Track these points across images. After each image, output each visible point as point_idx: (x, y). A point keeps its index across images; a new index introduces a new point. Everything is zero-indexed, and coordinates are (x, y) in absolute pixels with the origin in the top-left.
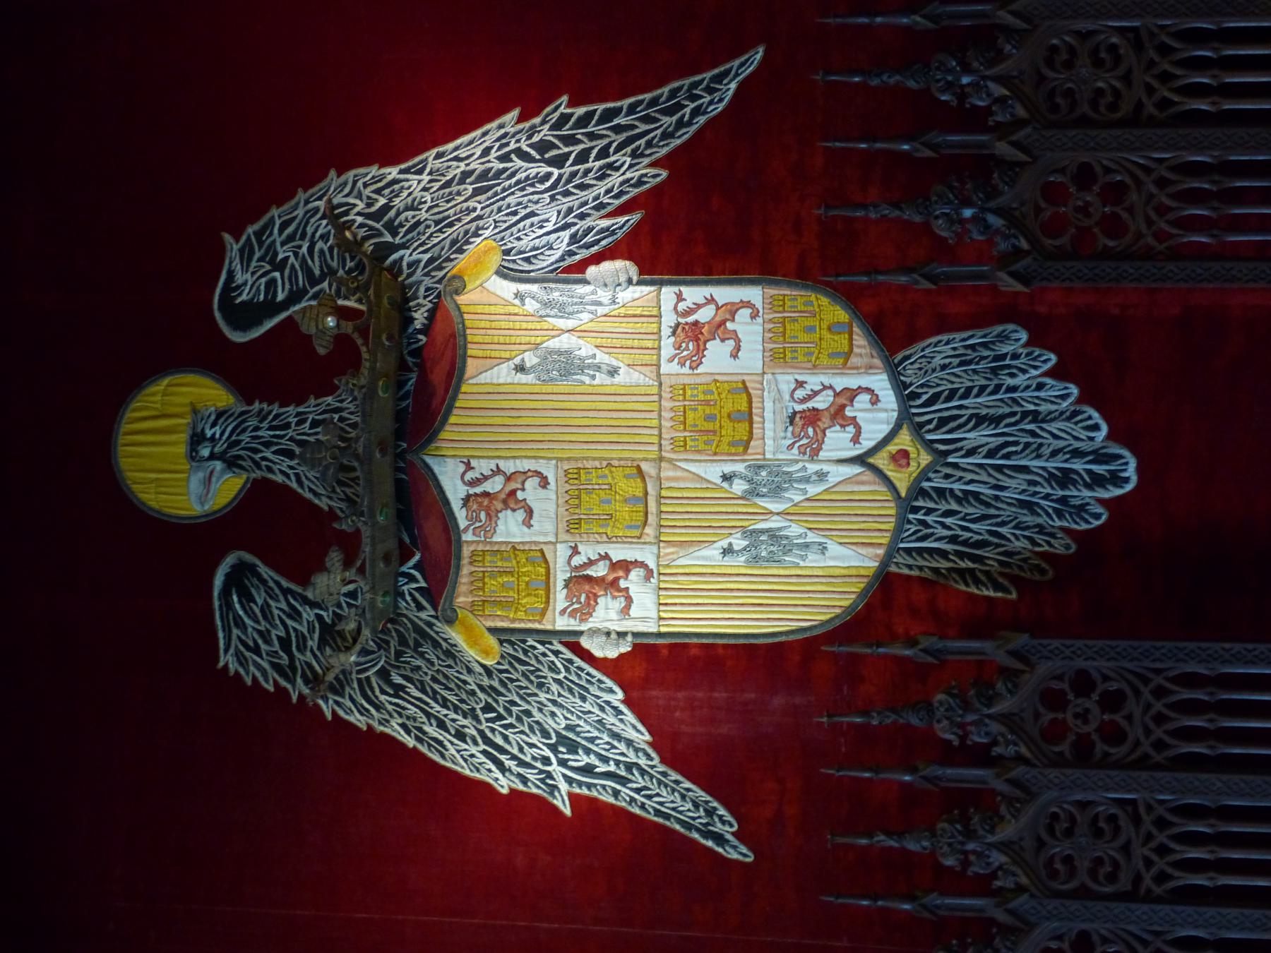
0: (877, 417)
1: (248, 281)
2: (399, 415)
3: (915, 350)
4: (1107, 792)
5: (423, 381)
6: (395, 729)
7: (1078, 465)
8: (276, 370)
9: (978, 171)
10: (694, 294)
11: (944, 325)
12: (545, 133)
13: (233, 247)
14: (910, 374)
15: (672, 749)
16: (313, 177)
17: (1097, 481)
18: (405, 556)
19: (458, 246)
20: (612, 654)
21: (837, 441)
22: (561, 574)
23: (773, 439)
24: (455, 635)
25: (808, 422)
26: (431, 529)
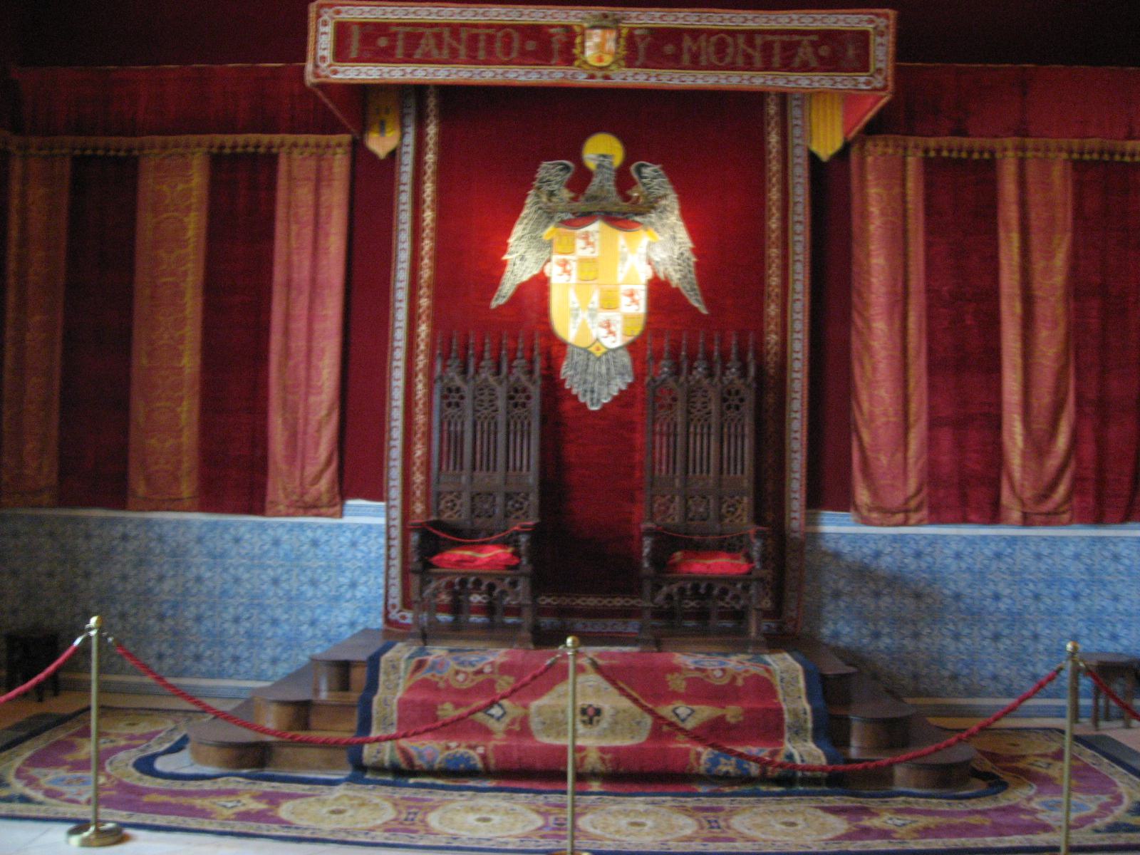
5: (620, 220)
6: (525, 211)
7: (595, 395)
8: (624, 180)
11: (634, 360)
13: (657, 167)
14: (621, 352)
15: (522, 288)
17: (592, 399)
18: (574, 214)
19: (656, 230)
21: (603, 332)
24: (551, 228)
25: (608, 325)
26: (581, 221)
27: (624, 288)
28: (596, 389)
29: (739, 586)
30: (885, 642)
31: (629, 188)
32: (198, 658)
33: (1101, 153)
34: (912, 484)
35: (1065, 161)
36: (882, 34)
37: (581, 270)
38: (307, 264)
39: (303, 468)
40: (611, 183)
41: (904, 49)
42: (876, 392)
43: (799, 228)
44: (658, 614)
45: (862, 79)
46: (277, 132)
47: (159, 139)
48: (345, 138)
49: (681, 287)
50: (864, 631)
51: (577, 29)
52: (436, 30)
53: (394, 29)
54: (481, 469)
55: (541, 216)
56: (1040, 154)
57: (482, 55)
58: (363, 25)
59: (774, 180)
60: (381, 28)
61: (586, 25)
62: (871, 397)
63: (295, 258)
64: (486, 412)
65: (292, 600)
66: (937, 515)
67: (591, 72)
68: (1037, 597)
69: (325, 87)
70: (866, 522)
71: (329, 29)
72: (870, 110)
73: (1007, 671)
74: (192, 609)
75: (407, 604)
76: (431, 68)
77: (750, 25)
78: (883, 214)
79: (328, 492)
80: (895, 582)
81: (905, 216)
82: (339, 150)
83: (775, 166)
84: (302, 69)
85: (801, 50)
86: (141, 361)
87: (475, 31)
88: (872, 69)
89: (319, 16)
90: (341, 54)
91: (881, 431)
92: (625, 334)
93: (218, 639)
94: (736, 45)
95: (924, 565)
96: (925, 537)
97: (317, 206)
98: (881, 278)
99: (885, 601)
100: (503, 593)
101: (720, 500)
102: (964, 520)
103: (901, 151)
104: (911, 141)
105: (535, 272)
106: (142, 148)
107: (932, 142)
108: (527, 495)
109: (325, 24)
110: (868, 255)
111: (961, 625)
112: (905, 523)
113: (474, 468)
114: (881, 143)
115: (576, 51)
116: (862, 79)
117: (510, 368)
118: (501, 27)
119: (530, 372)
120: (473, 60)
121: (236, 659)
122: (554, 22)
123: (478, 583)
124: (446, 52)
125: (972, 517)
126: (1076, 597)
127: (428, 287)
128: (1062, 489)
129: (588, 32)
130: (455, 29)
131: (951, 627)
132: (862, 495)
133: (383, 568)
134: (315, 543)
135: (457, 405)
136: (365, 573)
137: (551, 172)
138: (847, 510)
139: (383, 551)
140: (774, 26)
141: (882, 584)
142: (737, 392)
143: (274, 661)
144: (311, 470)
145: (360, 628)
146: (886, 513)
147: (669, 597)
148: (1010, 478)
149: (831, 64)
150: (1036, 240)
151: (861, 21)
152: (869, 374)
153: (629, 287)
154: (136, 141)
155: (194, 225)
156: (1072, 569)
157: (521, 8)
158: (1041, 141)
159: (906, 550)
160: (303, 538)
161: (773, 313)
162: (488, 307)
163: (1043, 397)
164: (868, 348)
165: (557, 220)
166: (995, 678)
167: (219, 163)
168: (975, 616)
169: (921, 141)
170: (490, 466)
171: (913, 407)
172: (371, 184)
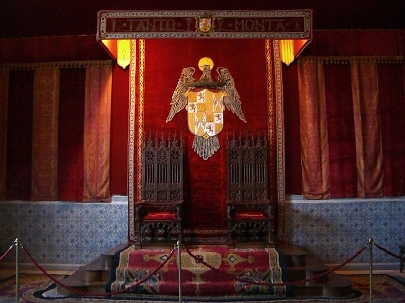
0: (211, 134)
1: (223, 71)
2: (210, 86)
3: (217, 138)
8: (213, 73)
10: (222, 116)
11: (219, 141)
12: (238, 101)
13: (226, 69)
18: (196, 87)
21: (208, 130)
22: (194, 103)
23: (207, 124)
24: (188, 92)
26: (198, 90)
28: (206, 152)
31: (216, 76)
32: (58, 256)
33: (388, 61)
37: (199, 107)
39: (97, 184)
40: (210, 75)
41: (317, 24)
45: (302, 35)
46: (85, 60)
49: (236, 113)
50: (308, 240)
51: (196, 18)
52: (144, 20)
53: (128, 20)
54: (161, 182)
57: (161, 29)
58: (117, 19)
59: (270, 73)
61: (200, 17)
62: (308, 152)
64: (163, 161)
65: (93, 234)
67: (201, 34)
70: (308, 199)
74: (56, 237)
77: (260, 16)
78: (309, 85)
79: (106, 192)
80: (319, 220)
82: (108, 66)
84: (95, 36)
85: (279, 25)
88: (305, 31)
89: (101, 16)
91: (312, 165)
92: (216, 131)
93: (66, 249)
94: (255, 23)
96: (329, 204)
98: (310, 108)
100: (171, 229)
102: (344, 197)
103: (315, 62)
104: (319, 58)
106: (35, 68)
107: (327, 58)
108: (179, 192)
109: (103, 19)
110: (305, 100)
112: (322, 199)
113: (158, 182)
115: (196, 26)
116: (302, 35)
117: (171, 144)
118: (168, 18)
119: (179, 146)
120: (158, 30)
121: (72, 256)
122: (188, 16)
123: (161, 225)
124: (148, 28)
125: (347, 196)
127: (142, 115)
128: (380, 184)
129: (200, 19)
130: (151, 19)
132: (306, 189)
133: (127, 221)
134: (101, 212)
135: (152, 158)
136: (120, 222)
137: (187, 72)
138: (301, 194)
139: (127, 214)
140: (269, 16)
141: (314, 222)
143: (87, 256)
145: (119, 243)
146: (313, 194)
151: (300, 14)
153: (217, 113)
155: (55, 94)
158: (366, 57)
159: (322, 209)
160: (97, 210)
161: (271, 122)
162: (165, 122)
163: (371, 151)
164: (307, 135)
167: (63, 72)
170: (165, 181)
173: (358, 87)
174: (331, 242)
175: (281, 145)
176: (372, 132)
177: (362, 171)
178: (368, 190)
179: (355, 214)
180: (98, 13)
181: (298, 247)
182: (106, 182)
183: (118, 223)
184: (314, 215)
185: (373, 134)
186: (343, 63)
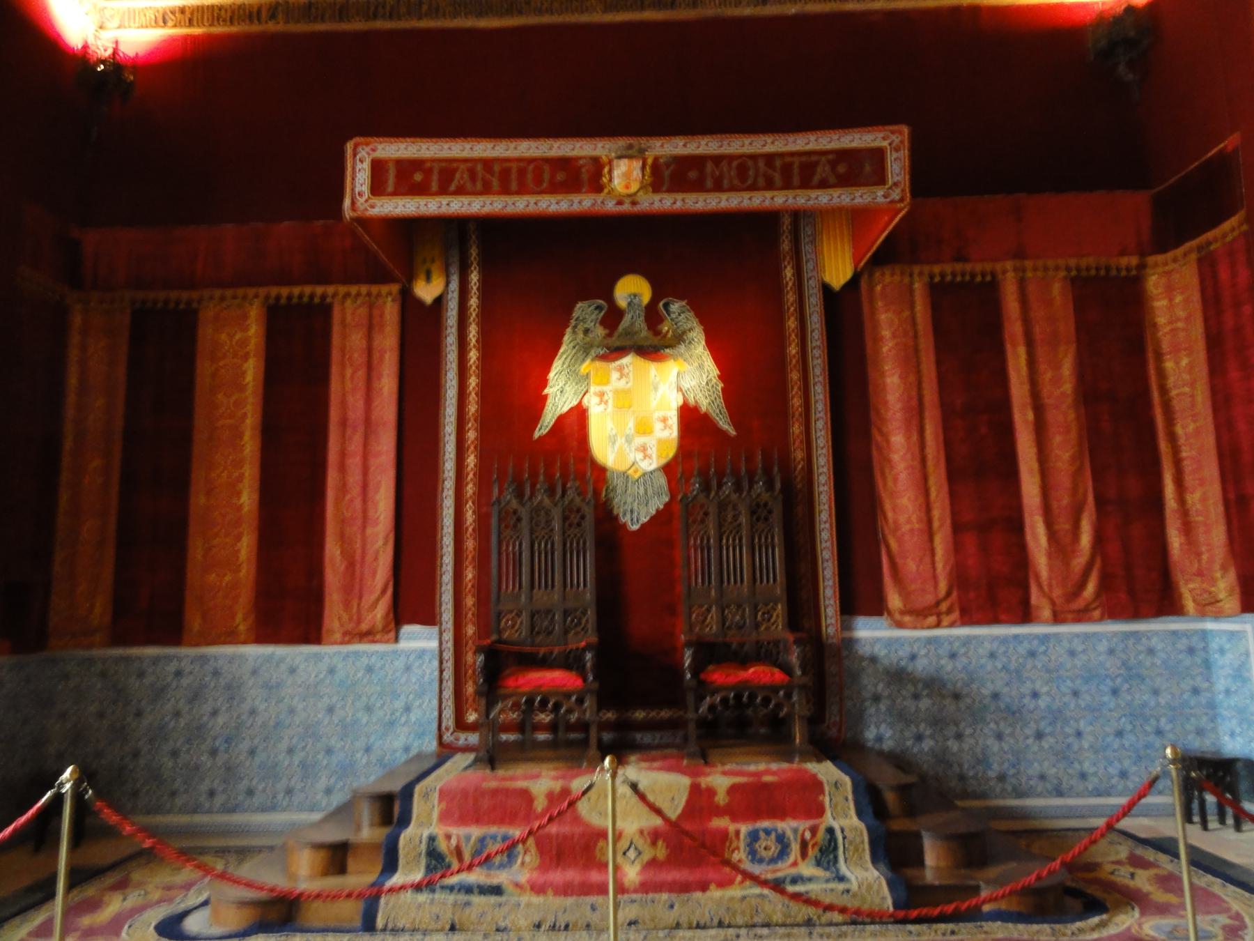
1: (675, 307)
4: (556, 525)
8: (653, 316)
9: (706, 488)
11: (669, 482)
13: (684, 303)
15: (561, 420)
16: (702, 322)
20: (585, 402)
21: (639, 456)
23: (639, 440)
24: (588, 362)
25: (644, 449)
26: (613, 356)
27: (656, 415)
29: (781, 693)
30: (927, 744)
33: (1098, 269)
34: (943, 586)
35: (1065, 278)
36: (897, 150)
38: (360, 404)
39: (360, 598)
40: (642, 318)
42: (899, 501)
43: (817, 353)
44: (702, 723)
45: (880, 193)
47: (218, 293)
48: (395, 288)
51: (605, 159)
52: (469, 165)
53: (428, 165)
55: (578, 351)
56: (1040, 274)
57: (514, 186)
58: (399, 162)
60: (417, 164)
63: (350, 399)
66: (968, 618)
68: (1076, 694)
69: (364, 222)
70: (900, 625)
71: (366, 165)
72: (883, 232)
73: (1054, 770)
75: (461, 725)
76: (465, 200)
78: (894, 336)
80: (933, 685)
81: (916, 336)
83: (791, 297)
85: (819, 169)
86: (198, 500)
87: (508, 164)
89: (355, 155)
90: (377, 188)
91: (907, 538)
92: (659, 457)
95: (959, 666)
96: (958, 638)
97: (369, 350)
98: (897, 395)
99: (925, 703)
101: (755, 609)
102: (995, 621)
103: (906, 280)
104: (916, 269)
105: (575, 403)
106: (200, 301)
107: (937, 269)
109: (361, 161)
110: (883, 374)
111: (1002, 724)
112: (938, 625)
114: (888, 273)
115: (605, 180)
116: (880, 193)
118: (531, 160)
120: (505, 190)
125: (1003, 617)
126: (1115, 692)
129: (615, 162)
130: (488, 163)
131: (992, 725)
132: (894, 600)
134: (370, 669)
137: (586, 312)
139: (436, 673)
141: (920, 686)
142: (766, 505)
143: (328, 791)
144: (369, 599)
146: (920, 614)
147: (712, 708)
148: (1037, 577)
149: (846, 181)
150: (1041, 352)
152: (890, 483)
154: (195, 295)
155: (252, 371)
156: (1108, 665)
157: (550, 142)
158: (1040, 263)
163: (1063, 500)
164: (889, 461)
165: (593, 353)
166: (1042, 777)
168: (1014, 714)
169: (926, 269)
171: (936, 513)
172: (421, 327)
173: (1020, 337)
174: (968, 742)
175: (826, 488)
176: (1064, 451)
177: (1043, 552)
178: (1059, 601)
179: (1029, 666)
180: (349, 146)
181: (881, 753)
182: (384, 592)
183: (411, 697)
184: (920, 668)
185: (1066, 456)
186: (979, 279)
